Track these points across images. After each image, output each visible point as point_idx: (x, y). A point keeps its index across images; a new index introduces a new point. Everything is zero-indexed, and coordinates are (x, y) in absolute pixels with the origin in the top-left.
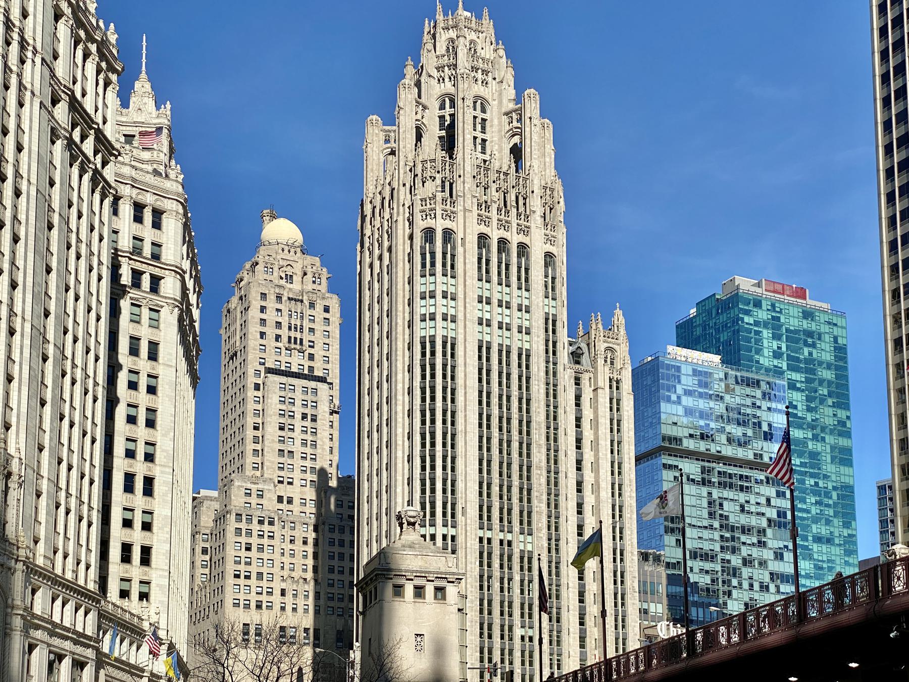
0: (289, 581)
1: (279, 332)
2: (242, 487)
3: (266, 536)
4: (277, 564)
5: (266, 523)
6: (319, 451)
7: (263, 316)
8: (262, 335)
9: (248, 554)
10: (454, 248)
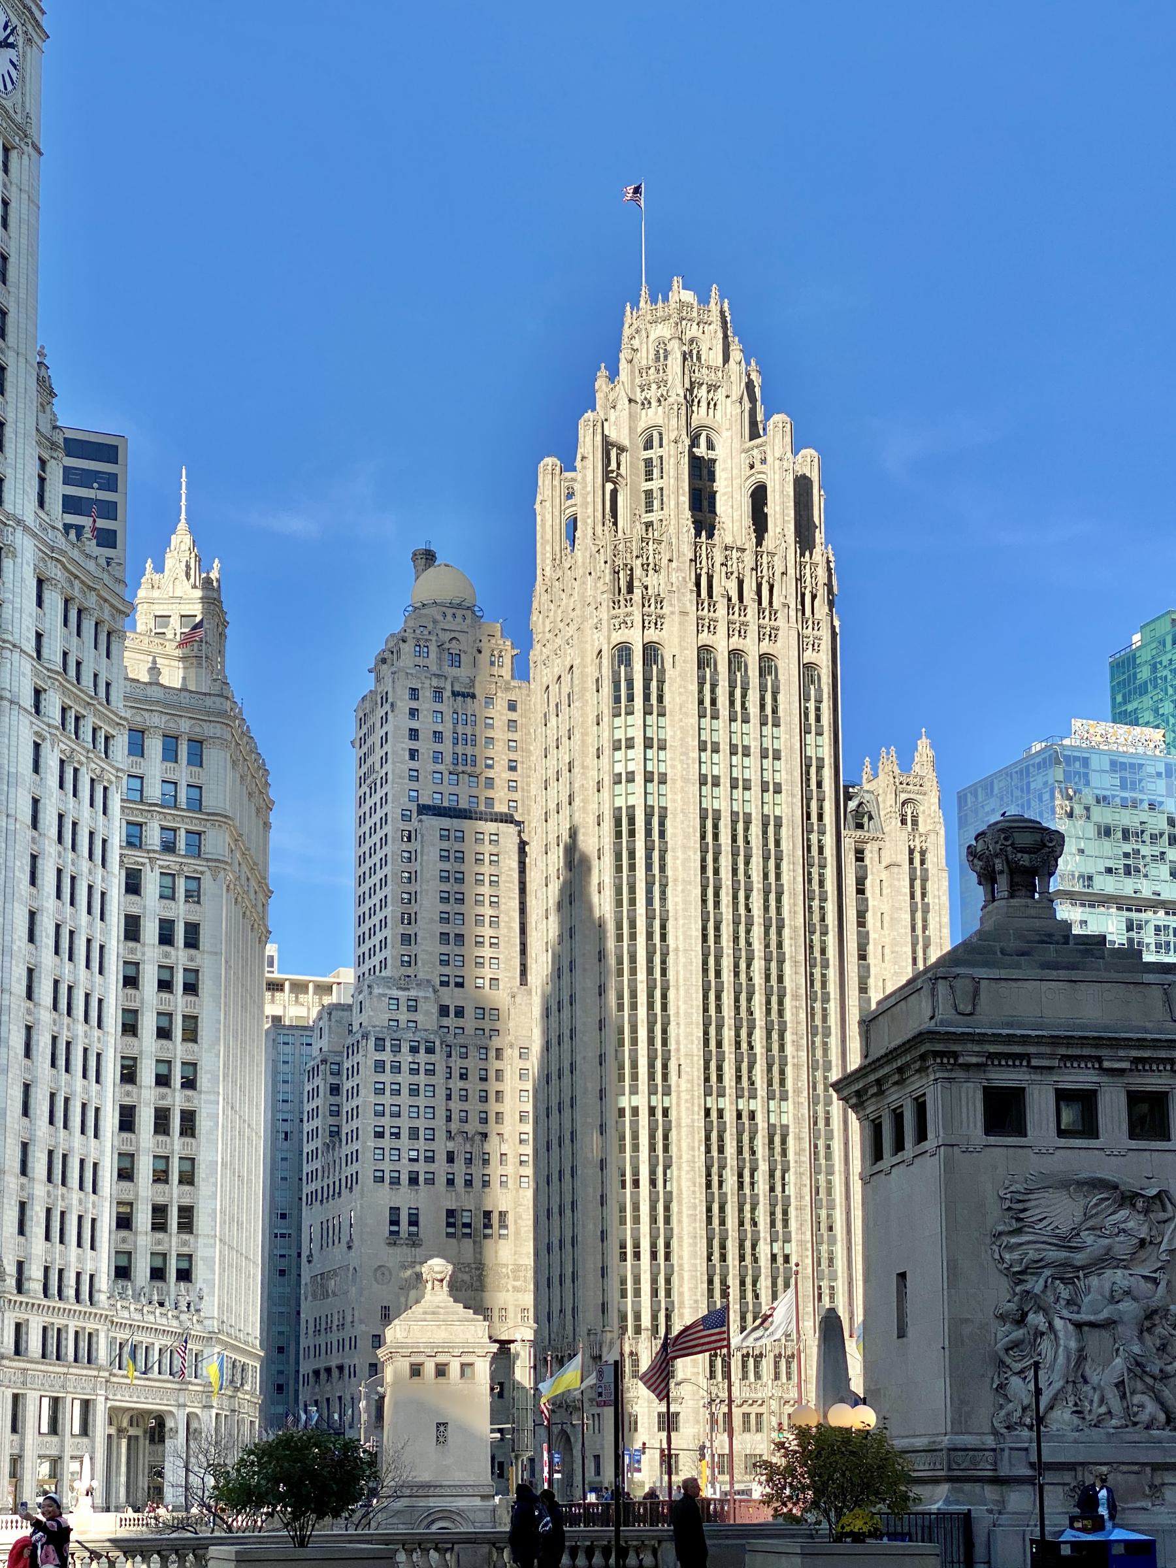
0: (459, 1139)
1: (439, 747)
2: (384, 995)
3: (422, 1071)
4: (441, 1113)
5: (422, 1051)
6: (503, 931)
7: (415, 725)
8: (413, 754)
9: (396, 1100)
10: (662, 672)
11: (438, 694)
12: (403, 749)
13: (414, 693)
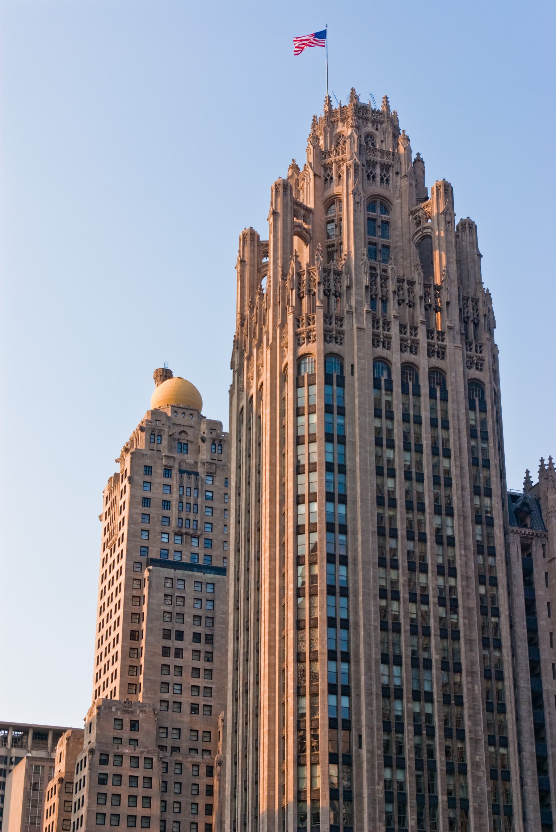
1: (166, 513)
7: (148, 495)
11: (168, 472)
12: (137, 514)
13: (148, 470)
